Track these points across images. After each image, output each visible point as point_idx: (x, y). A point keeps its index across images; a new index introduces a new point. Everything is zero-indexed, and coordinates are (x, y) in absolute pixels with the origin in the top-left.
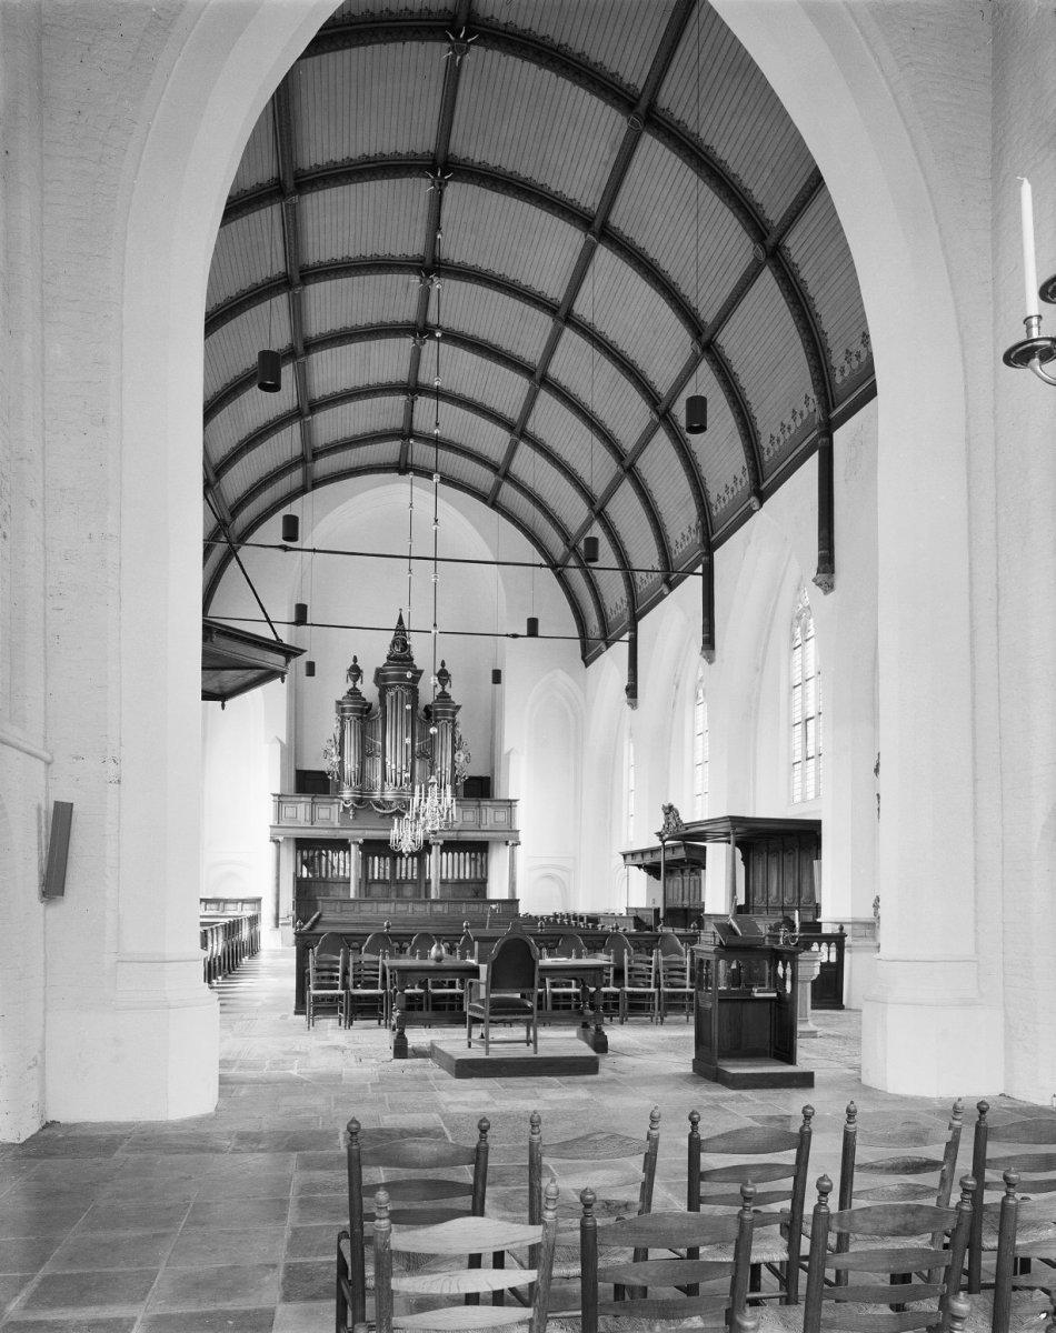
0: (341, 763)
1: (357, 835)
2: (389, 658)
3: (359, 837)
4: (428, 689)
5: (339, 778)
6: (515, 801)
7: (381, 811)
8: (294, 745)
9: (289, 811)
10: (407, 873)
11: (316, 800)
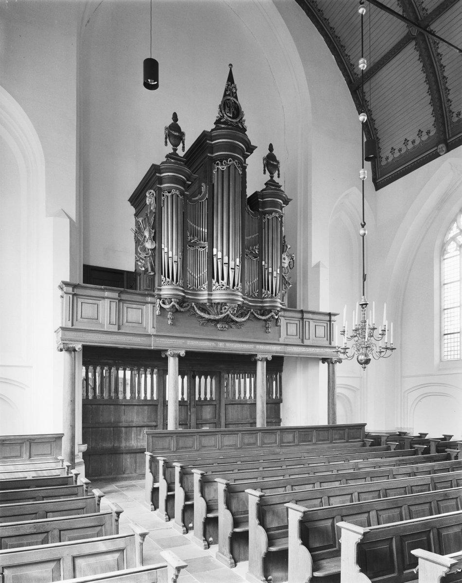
0: (157, 252)
1: (176, 345)
2: (217, 122)
3: (180, 348)
4: (256, 180)
5: (153, 270)
6: (335, 315)
7: (207, 316)
8: (82, 232)
9: (87, 309)
10: (206, 394)
11: (124, 297)
